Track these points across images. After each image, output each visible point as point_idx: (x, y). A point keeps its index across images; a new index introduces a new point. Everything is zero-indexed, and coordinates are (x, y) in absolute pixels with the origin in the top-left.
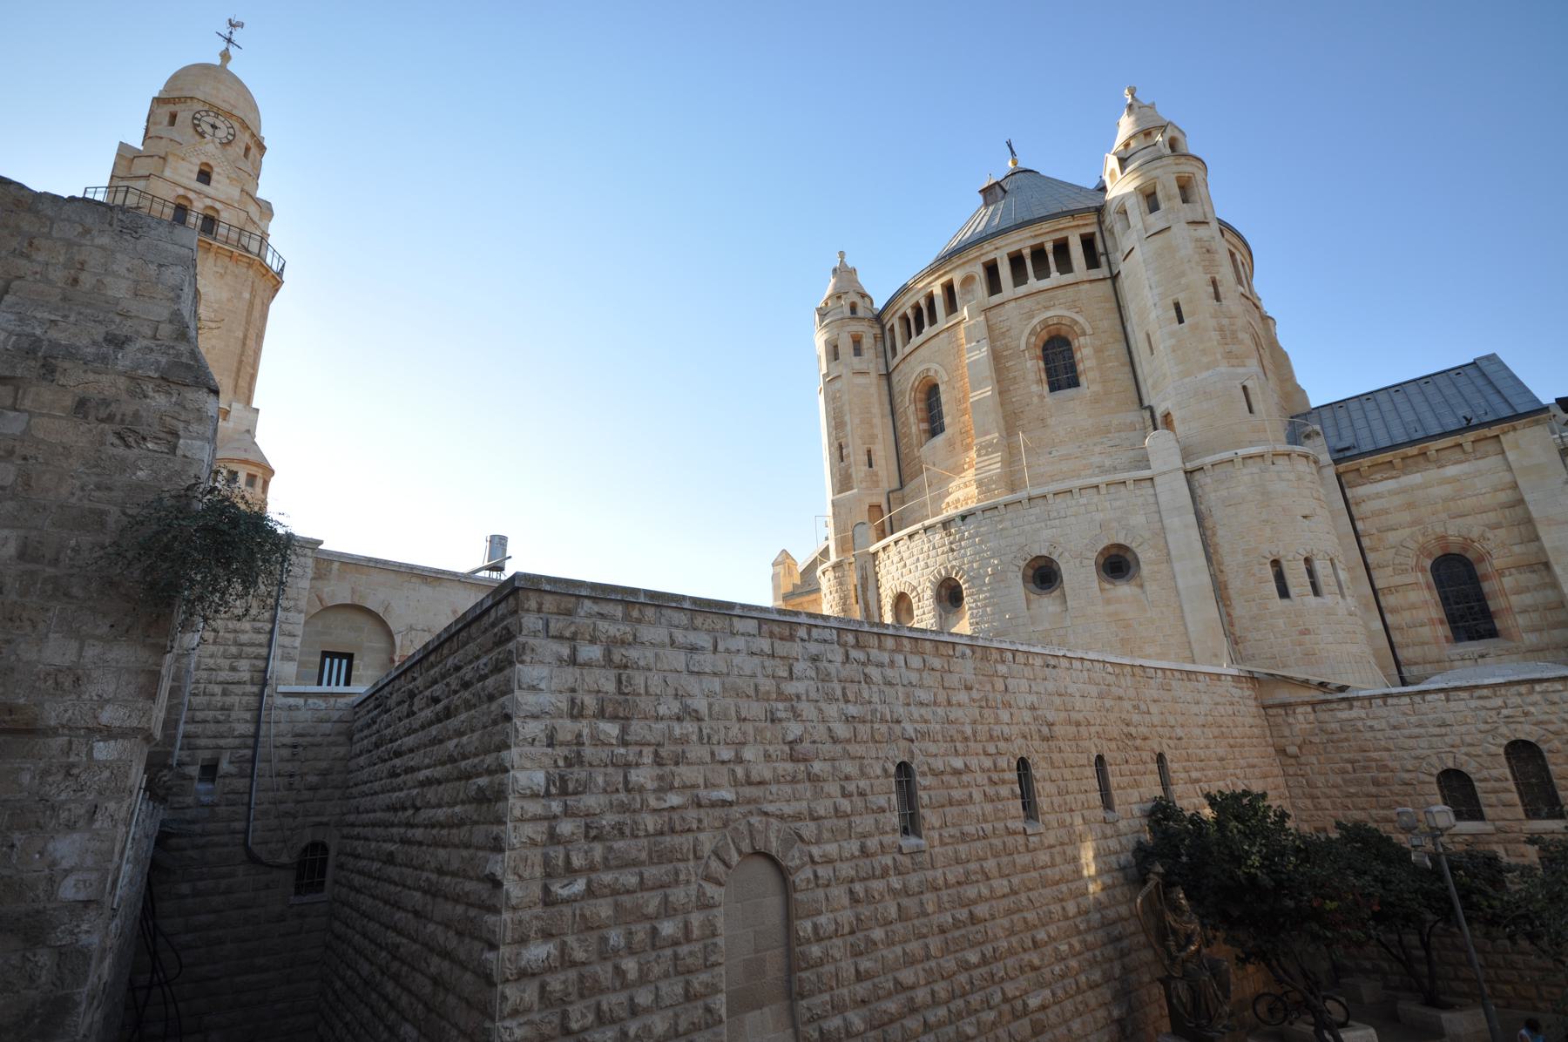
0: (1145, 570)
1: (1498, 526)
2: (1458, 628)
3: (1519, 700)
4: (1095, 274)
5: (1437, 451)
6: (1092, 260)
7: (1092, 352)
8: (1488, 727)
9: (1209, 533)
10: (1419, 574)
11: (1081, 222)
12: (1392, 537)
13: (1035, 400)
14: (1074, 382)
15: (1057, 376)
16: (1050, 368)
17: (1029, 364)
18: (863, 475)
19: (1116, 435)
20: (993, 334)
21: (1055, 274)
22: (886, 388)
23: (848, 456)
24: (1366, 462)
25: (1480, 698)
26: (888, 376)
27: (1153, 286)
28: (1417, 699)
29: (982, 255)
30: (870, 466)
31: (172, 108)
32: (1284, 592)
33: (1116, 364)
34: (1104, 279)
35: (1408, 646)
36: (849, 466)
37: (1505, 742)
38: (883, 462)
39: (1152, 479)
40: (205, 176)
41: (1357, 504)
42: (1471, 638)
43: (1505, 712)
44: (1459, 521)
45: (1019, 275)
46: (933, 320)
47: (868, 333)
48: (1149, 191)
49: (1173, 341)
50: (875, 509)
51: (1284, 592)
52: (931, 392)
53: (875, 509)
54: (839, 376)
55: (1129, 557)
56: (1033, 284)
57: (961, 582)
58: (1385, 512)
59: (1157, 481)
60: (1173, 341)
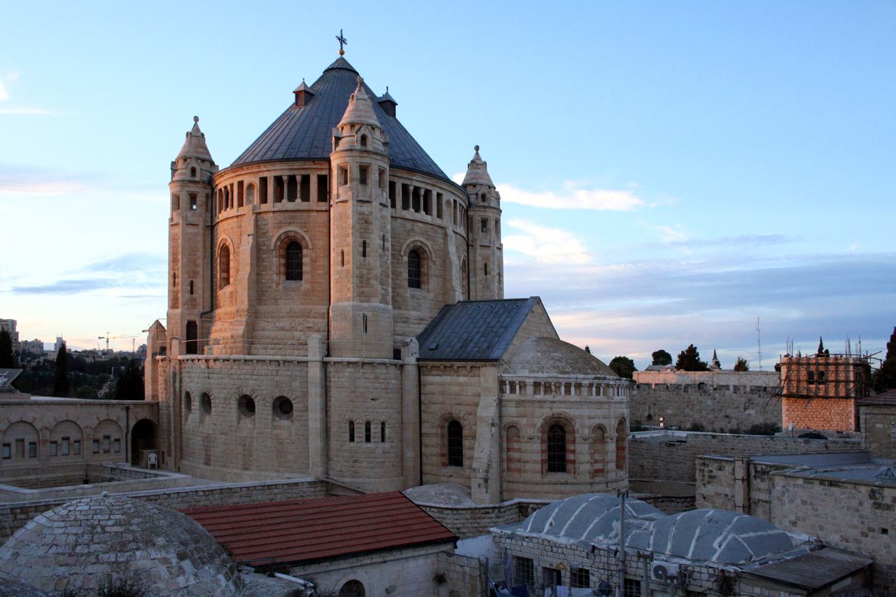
0: (295, 413)
5: (458, 367)
9: (328, 399)
10: (439, 430)
12: (434, 408)
15: (292, 269)
17: (275, 260)
18: (185, 299)
19: (313, 320)
24: (430, 363)
30: (192, 292)
32: (352, 439)
33: (322, 272)
38: (200, 292)
39: (307, 362)
41: (424, 385)
51: (352, 439)
58: (434, 394)
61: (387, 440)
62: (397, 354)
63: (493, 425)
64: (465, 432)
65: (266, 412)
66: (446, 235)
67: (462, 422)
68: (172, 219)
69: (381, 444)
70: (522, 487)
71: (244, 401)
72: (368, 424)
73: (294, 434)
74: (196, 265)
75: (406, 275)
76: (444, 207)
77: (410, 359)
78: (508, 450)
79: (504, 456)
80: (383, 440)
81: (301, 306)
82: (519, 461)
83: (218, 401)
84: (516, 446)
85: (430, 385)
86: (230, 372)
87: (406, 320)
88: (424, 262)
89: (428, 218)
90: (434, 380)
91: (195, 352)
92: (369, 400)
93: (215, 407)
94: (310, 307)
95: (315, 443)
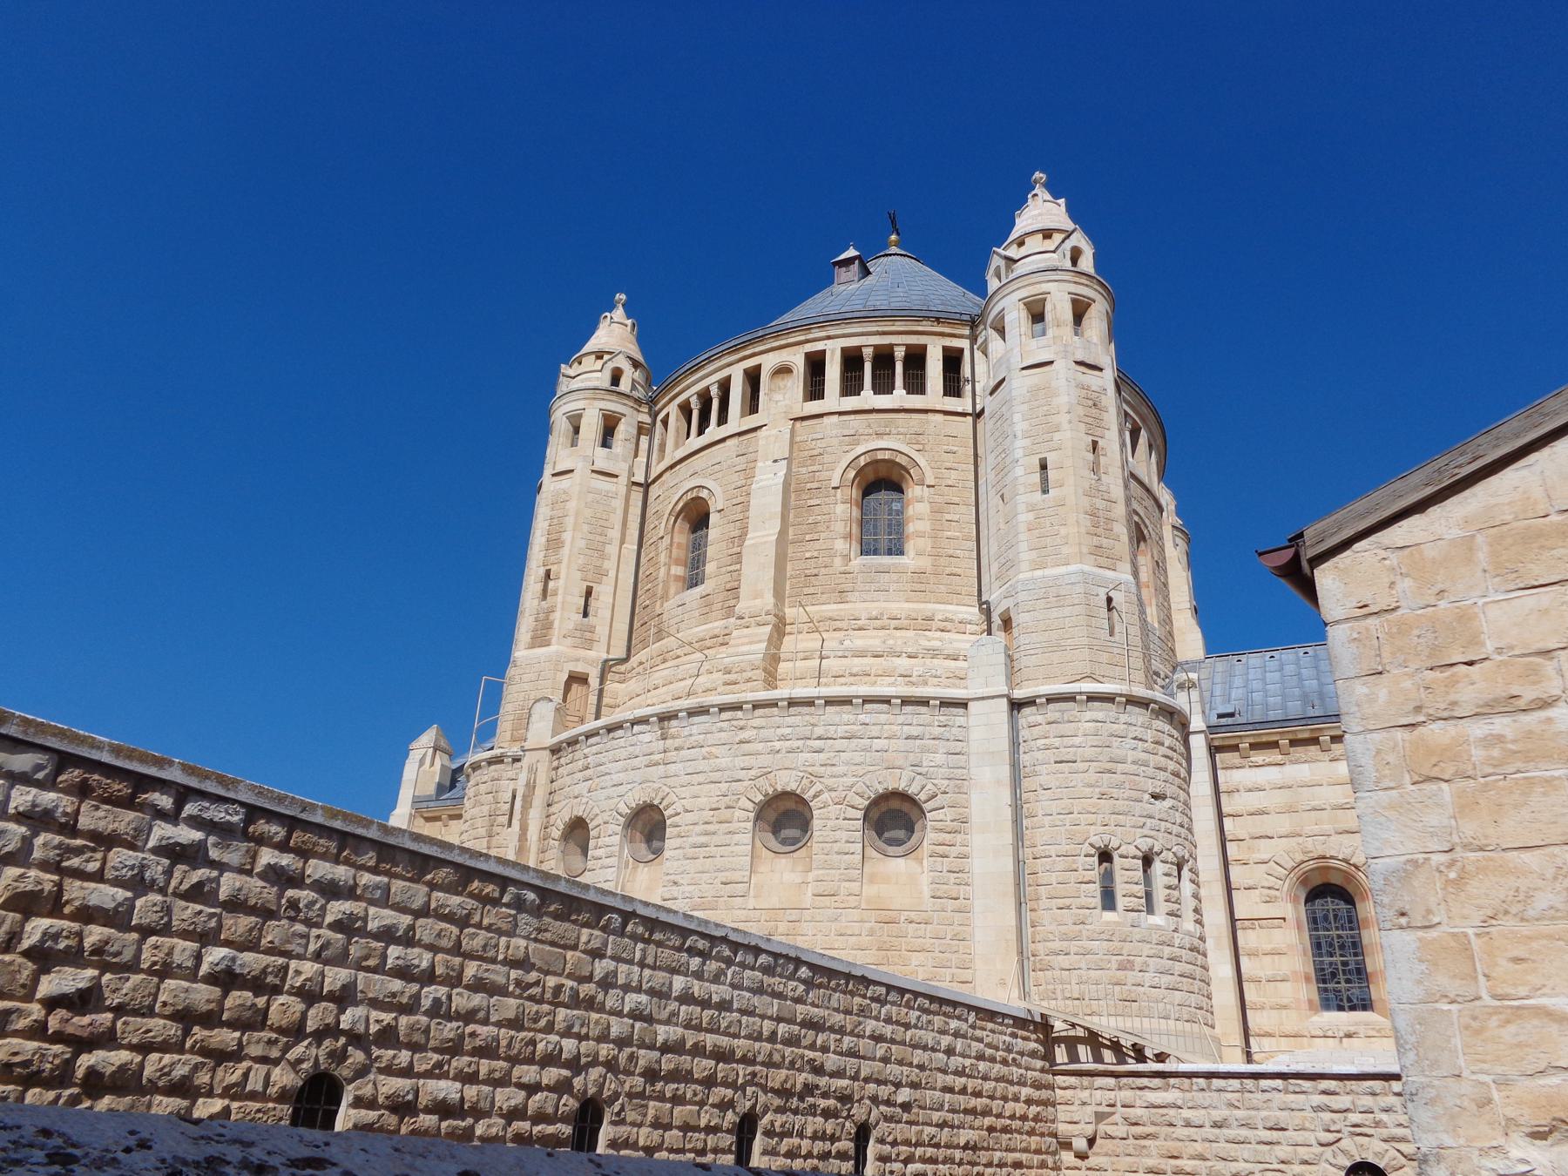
0: (931, 836)
2: (1326, 990)
3: (1367, 1101)
4: (952, 403)
6: (953, 386)
7: (928, 511)
8: (1331, 1137)
11: (947, 330)
12: (1265, 850)
13: (838, 561)
16: (868, 522)
18: (571, 626)
19: (939, 634)
21: (899, 391)
22: (640, 504)
23: (555, 594)
25: (1324, 1092)
26: (646, 486)
27: (1019, 434)
28: (1249, 1083)
29: (808, 341)
30: (585, 614)
32: (1108, 900)
34: (964, 415)
35: (1263, 1008)
36: (551, 610)
37: (1349, 1164)
39: (963, 704)
42: (1341, 1008)
43: (1355, 1118)
44: (1345, 838)
45: (851, 386)
46: (723, 420)
48: (1037, 310)
49: (1031, 516)
50: (577, 679)
51: (1108, 900)
54: (572, 471)
55: (914, 814)
56: (868, 398)
57: (666, 813)
60: (1031, 516)
65: (844, 835)
72: (1147, 861)
73: (927, 891)
74: (603, 556)
81: (906, 605)
83: (689, 817)
85: (1250, 790)
86: (737, 740)
92: (1147, 797)
93: (679, 836)
94: (930, 606)
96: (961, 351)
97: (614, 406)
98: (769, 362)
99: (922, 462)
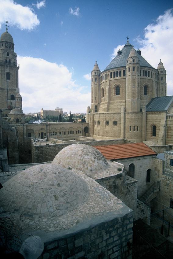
1: (158, 124)
14: (119, 94)
17: (114, 91)
20: (110, 85)
21: (119, 77)
26: (100, 85)
30: (96, 99)
31: (2, 43)
32: (130, 130)
38: (98, 99)
40: (8, 55)
45: (114, 77)
47: (97, 77)
51: (130, 130)
52: (103, 89)
53: (96, 107)
56: (116, 78)
58: (150, 119)
59: (121, 114)
61: (138, 130)
62: (141, 110)
63: (164, 126)
64: (157, 128)
66: (153, 81)
67: (156, 126)
68: (92, 84)
69: (137, 131)
70: (171, 142)
71: (107, 122)
72: (134, 126)
75: (143, 92)
76: (153, 75)
77: (144, 111)
78: (168, 132)
79: (167, 134)
80: (138, 130)
82: (170, 135)
84: (170, 132)
87: (143, 102)
88: (148, 89)
89: (149, 78)
90: (150, 116)
91: (97, 112)
95: (122, 131)
96: (125, 70)
97: (96, 77)
98: (107, 73)
99: (120, 85)
